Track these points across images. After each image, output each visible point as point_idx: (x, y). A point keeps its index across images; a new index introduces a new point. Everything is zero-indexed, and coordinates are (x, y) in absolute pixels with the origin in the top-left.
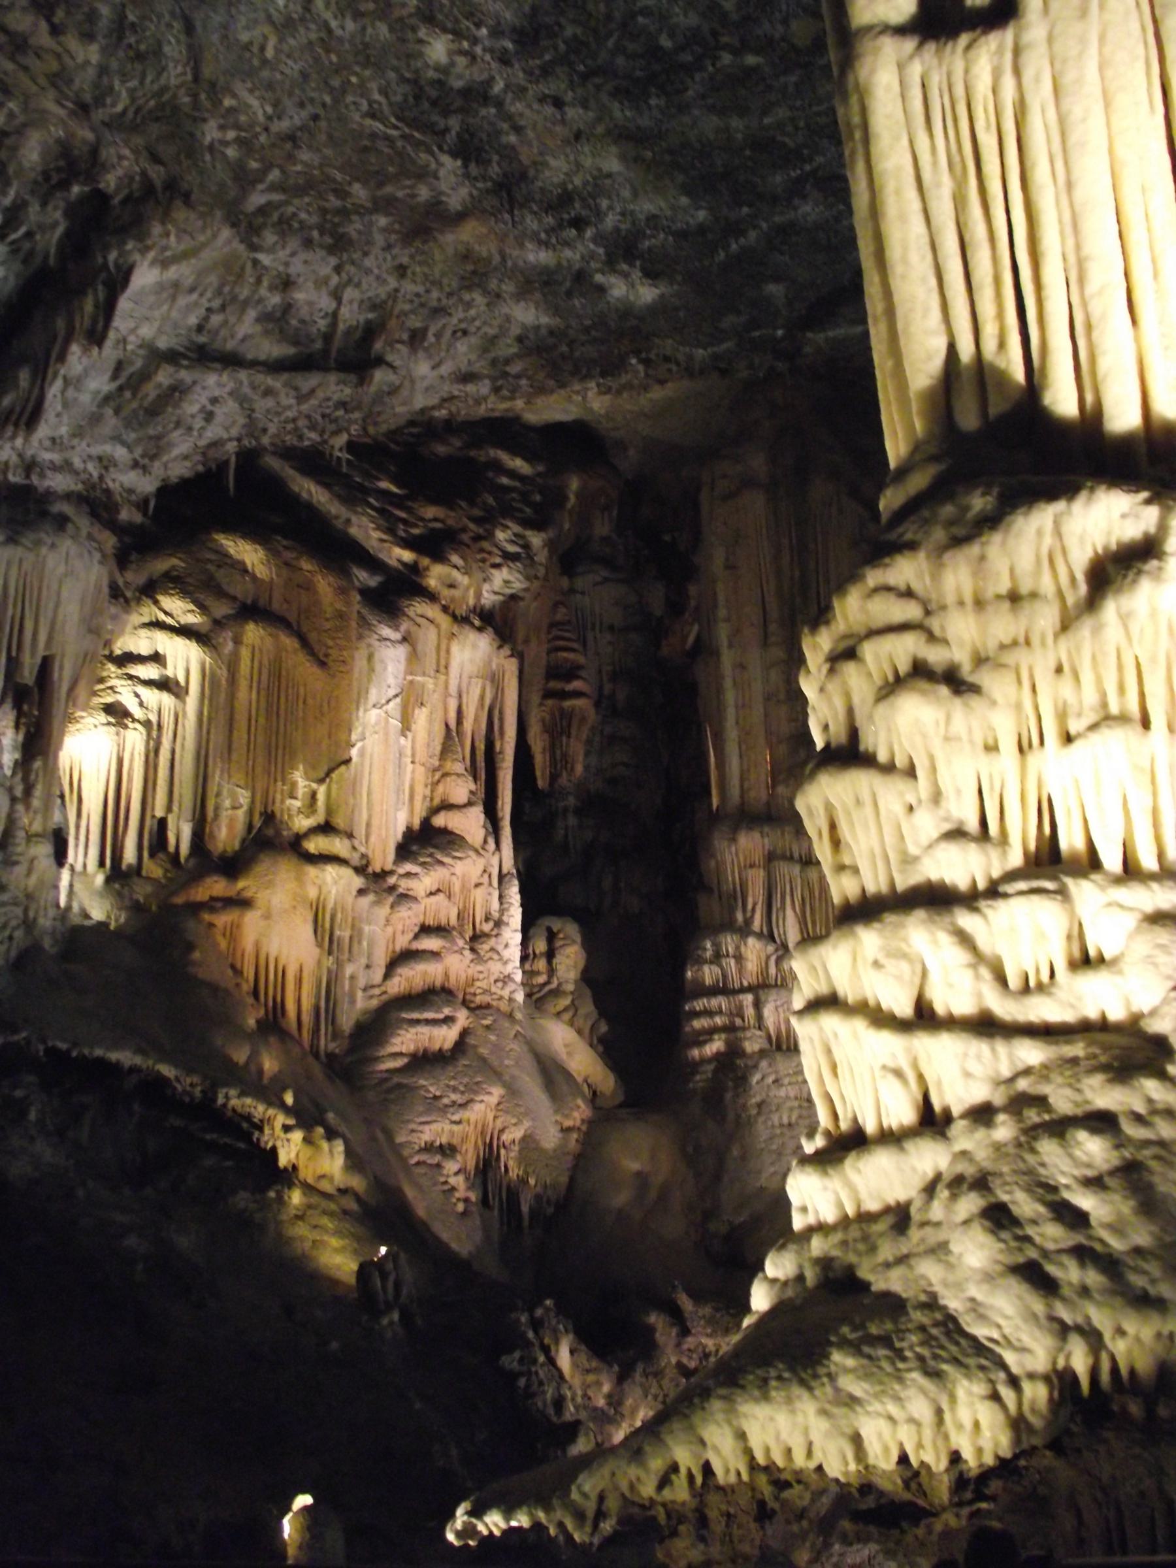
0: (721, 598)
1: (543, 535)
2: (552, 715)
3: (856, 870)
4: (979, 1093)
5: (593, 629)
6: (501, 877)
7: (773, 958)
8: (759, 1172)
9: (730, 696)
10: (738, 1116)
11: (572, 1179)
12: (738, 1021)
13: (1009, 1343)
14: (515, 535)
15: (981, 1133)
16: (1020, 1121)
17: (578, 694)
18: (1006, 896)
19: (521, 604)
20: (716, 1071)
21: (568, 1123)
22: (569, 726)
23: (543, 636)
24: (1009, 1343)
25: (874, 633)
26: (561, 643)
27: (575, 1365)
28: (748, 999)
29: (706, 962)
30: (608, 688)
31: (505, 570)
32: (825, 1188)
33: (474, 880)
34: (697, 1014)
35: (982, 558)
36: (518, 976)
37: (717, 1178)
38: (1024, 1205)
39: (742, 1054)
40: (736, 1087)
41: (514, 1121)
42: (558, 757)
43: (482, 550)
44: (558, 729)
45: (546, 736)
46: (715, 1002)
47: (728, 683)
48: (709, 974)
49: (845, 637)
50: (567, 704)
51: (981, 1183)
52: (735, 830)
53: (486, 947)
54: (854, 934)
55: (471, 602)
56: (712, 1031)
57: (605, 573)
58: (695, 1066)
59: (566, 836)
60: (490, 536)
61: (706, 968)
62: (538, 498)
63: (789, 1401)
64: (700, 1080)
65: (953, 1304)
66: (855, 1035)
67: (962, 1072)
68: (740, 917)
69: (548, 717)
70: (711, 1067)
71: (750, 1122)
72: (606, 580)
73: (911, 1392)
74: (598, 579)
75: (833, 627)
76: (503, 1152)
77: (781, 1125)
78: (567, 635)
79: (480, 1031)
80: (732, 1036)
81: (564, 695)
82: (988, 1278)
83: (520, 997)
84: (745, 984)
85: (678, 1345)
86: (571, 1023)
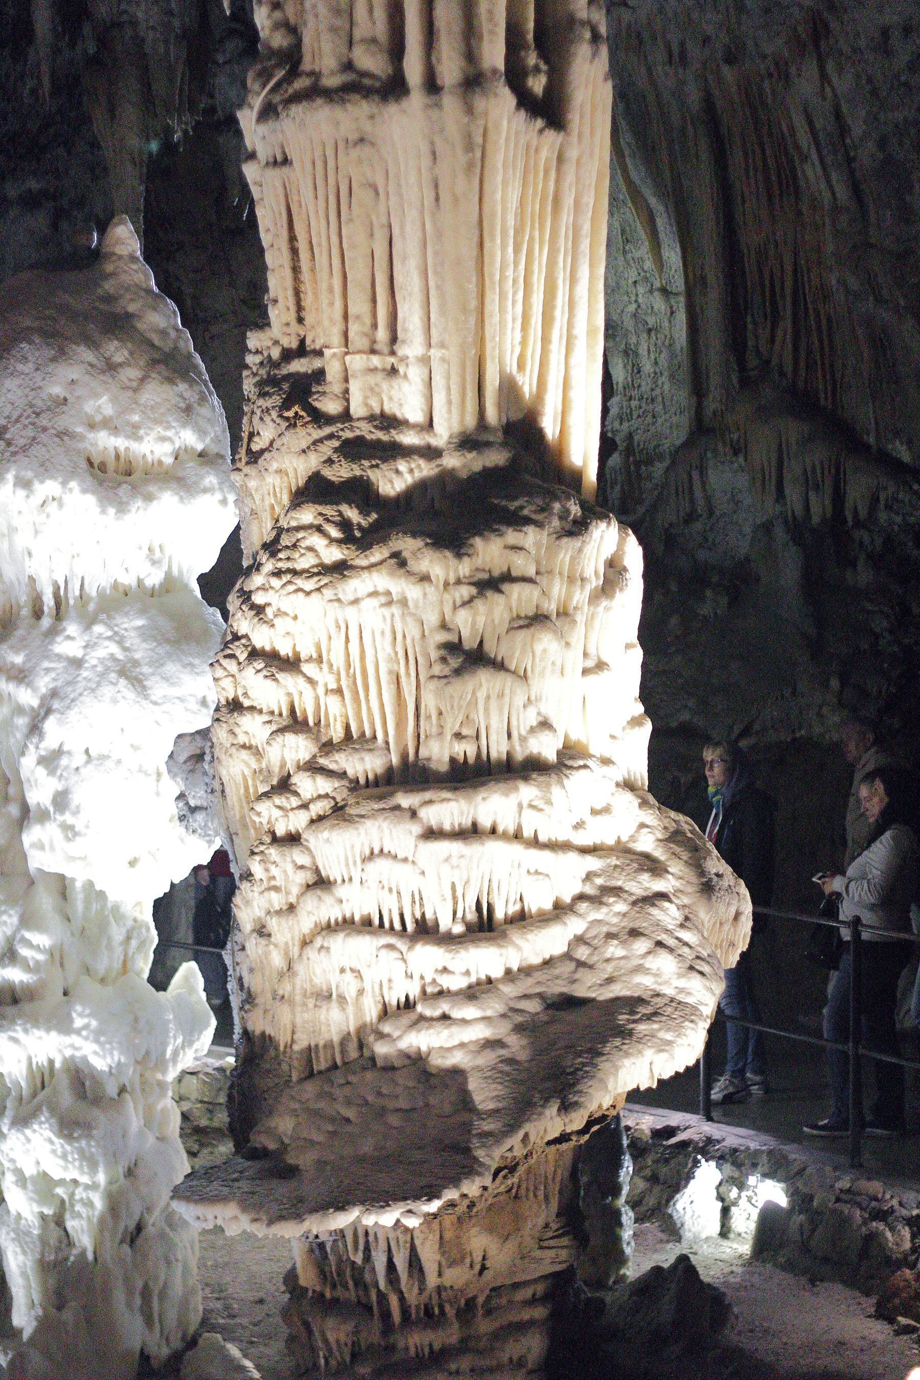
4: (577, 888)
13: (702, 1004)
15: (604, 910)
16: (625, 900)
18: (571, 768)
24: (702, 1004)
32: (501, 955)
35: (580, 550)
38: (671, 942)
51: (635, 933)
54: (517, 789)
63: (640, 1052)
65: (669, 991)
67: (567, 876)
73: (689, 1032)
82: (680, 976)
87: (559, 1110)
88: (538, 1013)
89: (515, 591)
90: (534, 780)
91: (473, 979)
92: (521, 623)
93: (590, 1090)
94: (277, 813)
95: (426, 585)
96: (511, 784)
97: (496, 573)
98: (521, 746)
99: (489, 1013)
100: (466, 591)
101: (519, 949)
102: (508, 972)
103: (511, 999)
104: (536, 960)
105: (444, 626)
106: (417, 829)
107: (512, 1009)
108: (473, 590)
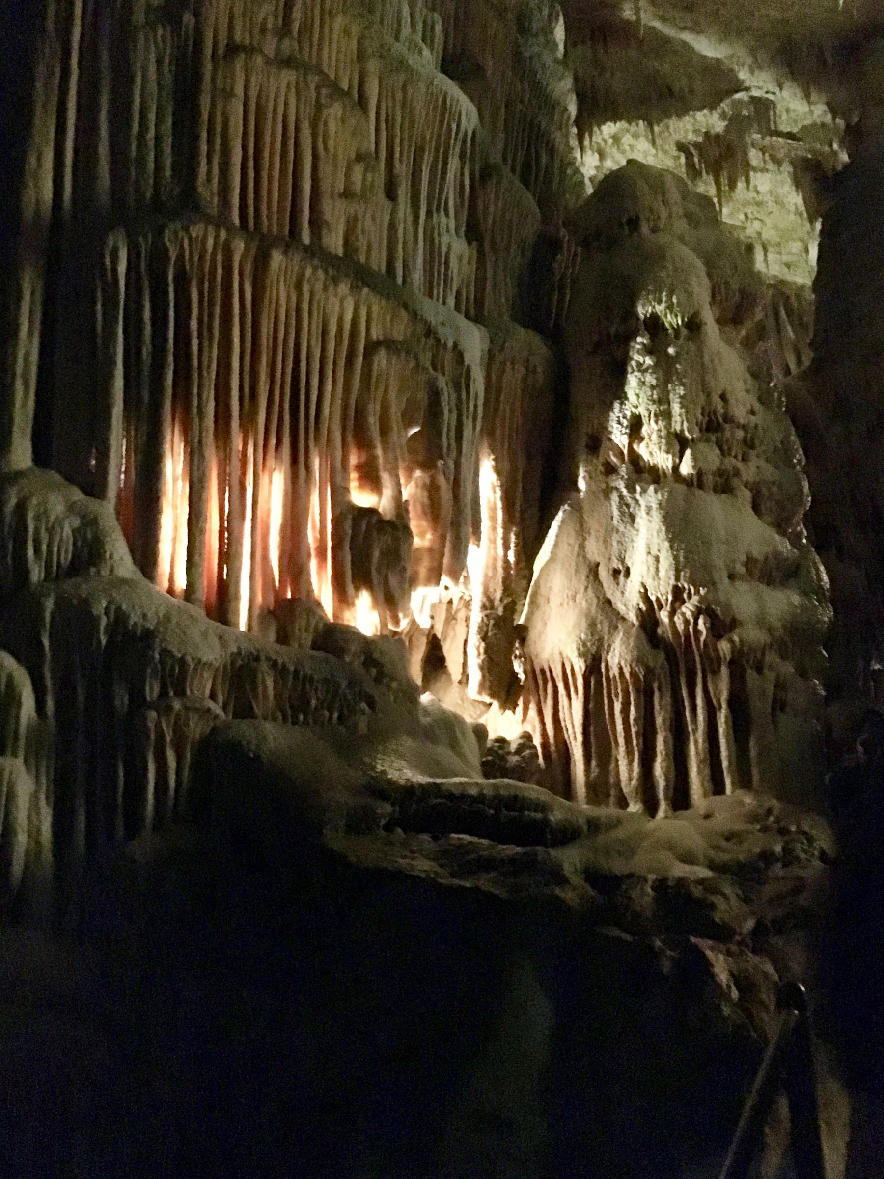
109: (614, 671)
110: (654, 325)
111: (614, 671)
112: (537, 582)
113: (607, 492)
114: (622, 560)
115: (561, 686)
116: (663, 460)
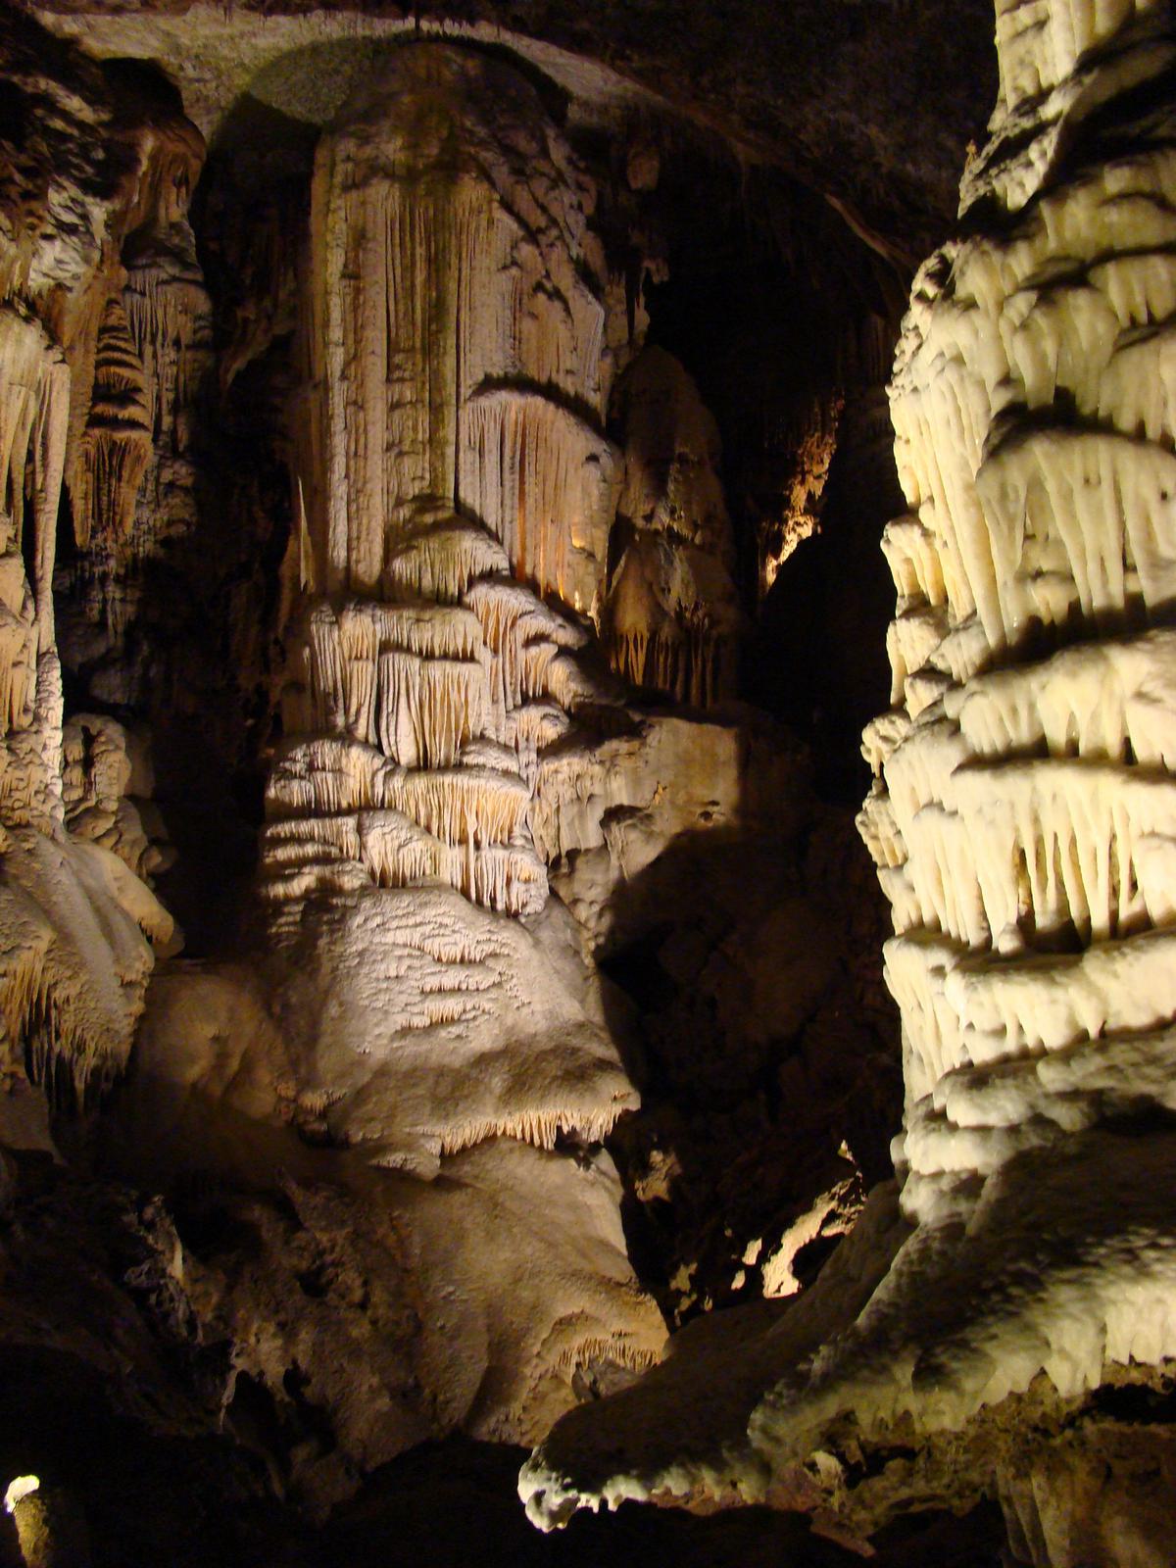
0: (336, 315)
1: (108, 205)
2: (99, 449)
3: (1068, 578)
5: (153, 342)
6: (40, 656)
7: (381, 774)
8: (362, 1034)
9: (339, 442)
10: (335, 969)
11: (134, 1047)
12: (334, 851)
14: (73, 200)
17: (133, 424)
19: (69, 295)
20: (304, 913)
21: (131, 976)
22: (121, 466)
23: (93, 345)
25: (1109, 255)
26: (117, 355)
27: (187, 1273)
28: (350, 822)
29: (294, 776)
30: (167, 421)
31: (58, 243)
32: (1054, 1002)
33: (12, 657)
34: (280, 842)
36: (58, 789)
37: (313, 1040)
39: (339, 891)
40: (332, 932)
41: (69, 973)
42: (104, 506)
43: (31, 213)
44: (107, 466)
45: (90, 475)
46: (304, 827)
47: (338, 425)
48: (298, 792)
49: (1053, 259)
50: (121, 436)
52: (339, 611)
53: (25, 747)
54: (1105, 659)
55: (17, 282)
56: (302, 863)
57: (174, 271)
58: (279, 906)
59: (103, 612)
60: (40, 195)
61: (295, 784)
62: (100, 155)
64: (287, 923)
66: (1094, 798)
68: (340, 721)
69: (93, 451)
70: (299, 908)
71: (351, 975)
72: (174, 279)
74: (164, 276)
75: (1038, 243)
76: (54, 1013)
77: (388, 978)
78: (122, 344)
79: (21, 857)
80: (327, 871)
81: (116, 424)
83: (60, 814)
84: (344, 804)
85: (287, 1243)
86: (114, 849)
87: (916, 1376)
88: (1072, 1134)
89: (1113, 280)
90: (1150, 640)
91: (1010, 1045)
92: (1136, 335)
93: (989, 1347)
94: (885, 747)
95: (973, 313)
96: (1088, 651)
97: (1090, 254)
98: (1155, 579)
99: (994, 1119)
100: (1022, 303)
101: (1094, 991)
102: (1082, 1037)
103: (1047, 1096)
104: (1139, 1019)
105: (1007, 380)
106: (954, 755)
107: (1038, 1120)
108: (1033, 296)
109: (663, 639)
110: (682, 459)
111: (663, 639)
112: (616, 588)
113: (656, 545)
114: (667, 583)
115: (631, 646)
116: (686, 532)
